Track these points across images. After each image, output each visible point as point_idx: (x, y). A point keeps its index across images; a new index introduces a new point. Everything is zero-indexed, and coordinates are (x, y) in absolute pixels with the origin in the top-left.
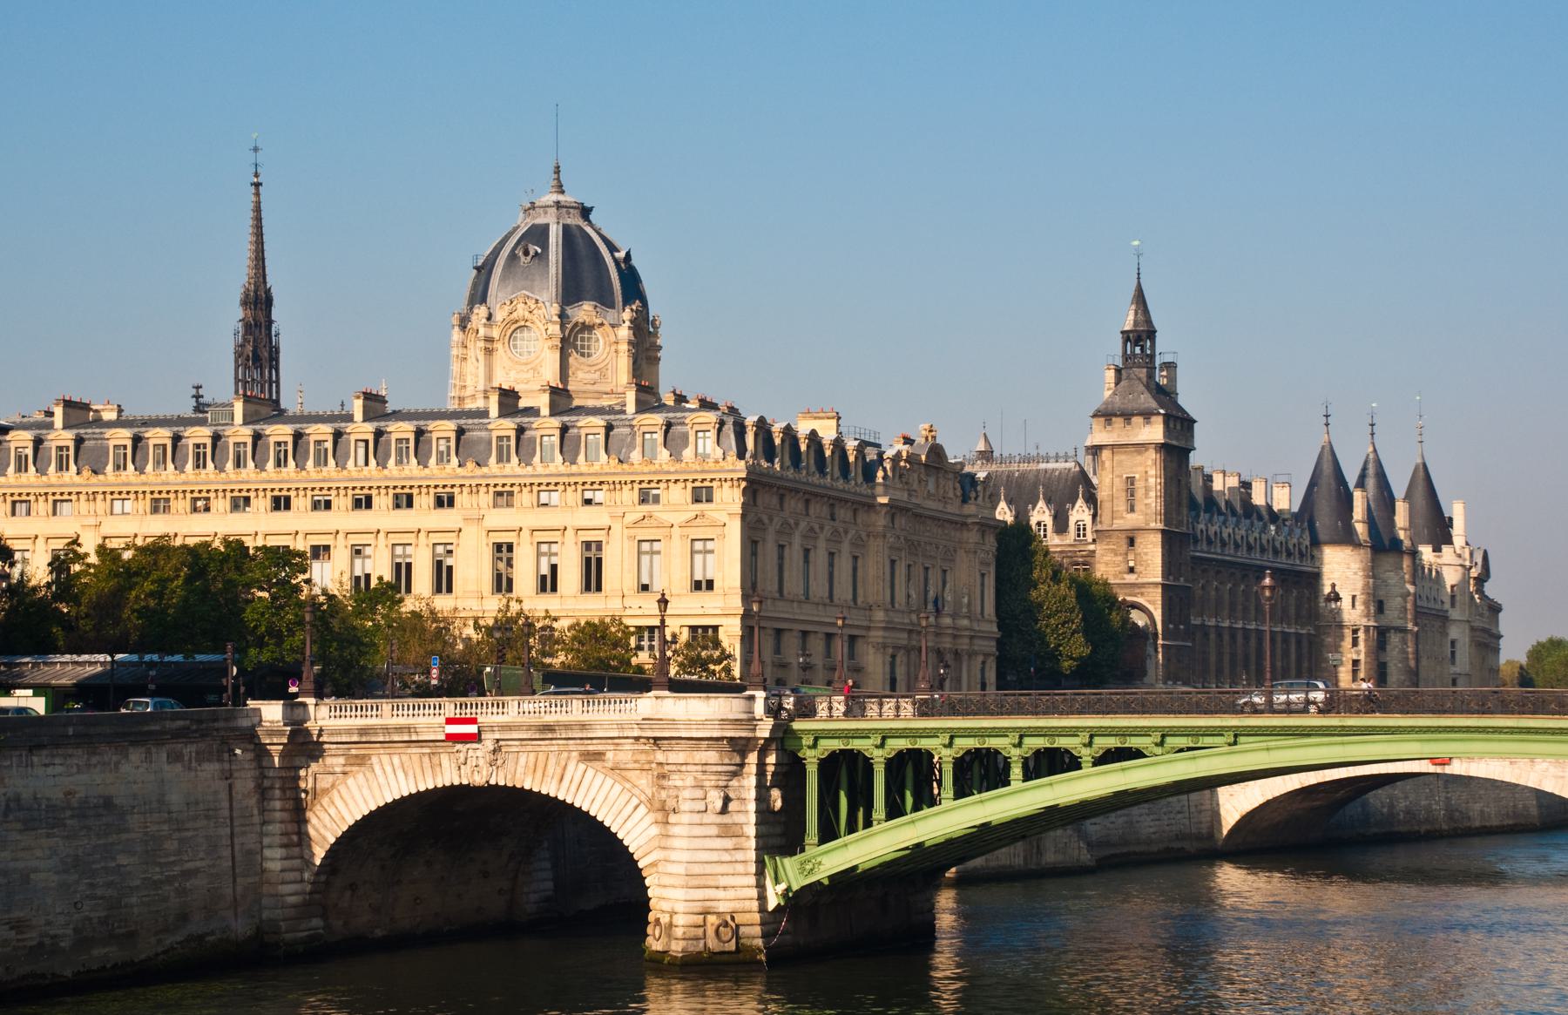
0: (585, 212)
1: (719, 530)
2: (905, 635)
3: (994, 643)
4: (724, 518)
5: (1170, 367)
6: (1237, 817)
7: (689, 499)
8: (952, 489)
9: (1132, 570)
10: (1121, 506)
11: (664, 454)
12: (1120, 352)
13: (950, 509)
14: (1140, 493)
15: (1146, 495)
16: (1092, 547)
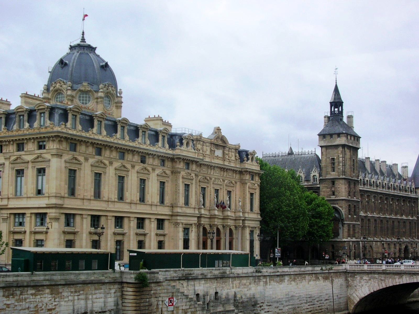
0: (92, 49)
1: (47, 164)
2: (196, 219)
3: (259, 223)
4: (48, 156)
5: (350, 117)
6: (358, 300)
7: (36, 148)
8: (233, 156)
9: (334, 195)
10: (330, 169)
11: (27, 125)
12: (330, 111)
13: (232, 165)
14: (336, 164)
15: (339, 165)
16: (318, 186)
